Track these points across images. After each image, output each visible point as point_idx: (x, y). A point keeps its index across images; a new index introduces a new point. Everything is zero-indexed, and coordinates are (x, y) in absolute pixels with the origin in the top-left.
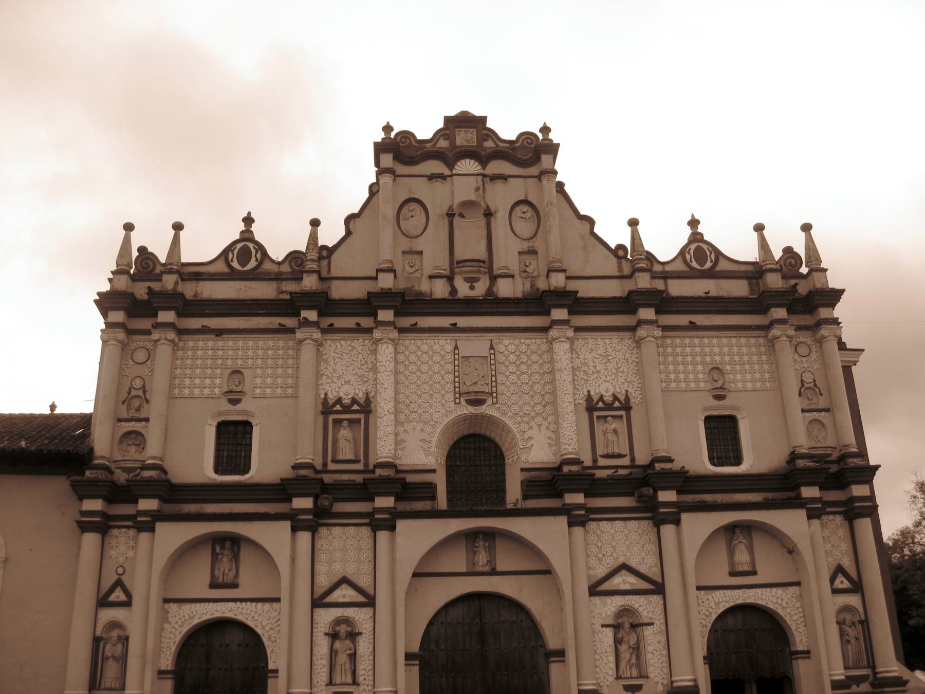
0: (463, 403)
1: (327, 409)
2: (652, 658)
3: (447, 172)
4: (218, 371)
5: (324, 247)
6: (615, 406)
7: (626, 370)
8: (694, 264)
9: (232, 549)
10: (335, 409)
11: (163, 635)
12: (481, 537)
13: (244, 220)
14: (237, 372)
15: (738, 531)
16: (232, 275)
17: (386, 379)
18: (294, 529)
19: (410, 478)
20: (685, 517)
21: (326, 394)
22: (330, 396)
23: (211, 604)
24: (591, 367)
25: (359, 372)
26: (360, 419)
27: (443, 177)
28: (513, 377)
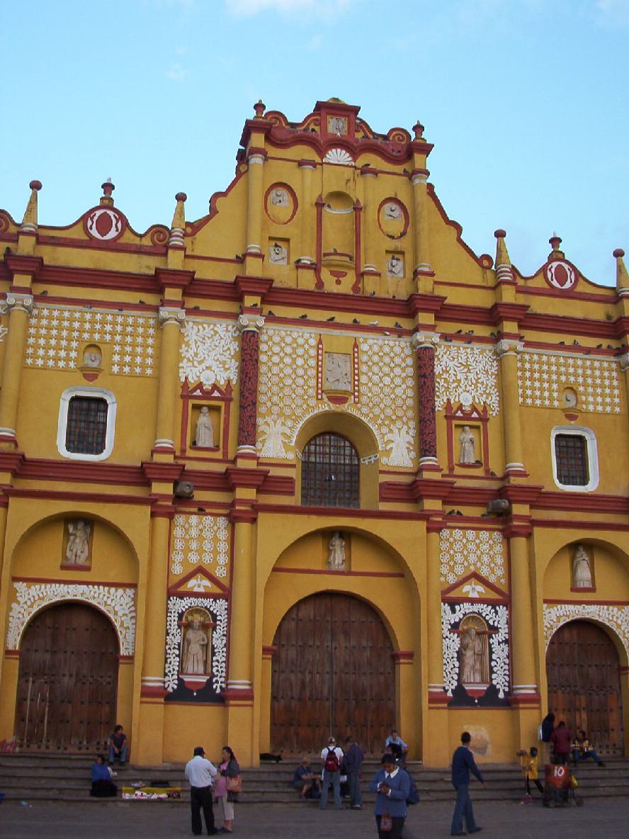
0: (326, 400)
1: (187, 392)
2: (496, 666)
3: (318, 160)
4: (74, 344)
5: (188, 224)
6: (473, 416)
7: (485, 383)
8: (555, 283)
9: (85, 531)
10: (195, 394)
11: (11, 614)
12: (337, 536)
13: (104, 186)
14: (93, 346)
15: (581, 549)
16: (91, 244)
18: (153, 515)
19: (274, 472)
20: (537, 531)
21: (186, 378)
22: (190, 379)
23: (62, 585)
24: (452, 375)
25: (222, 358)
26: (218, 409)
27: (314, 165)
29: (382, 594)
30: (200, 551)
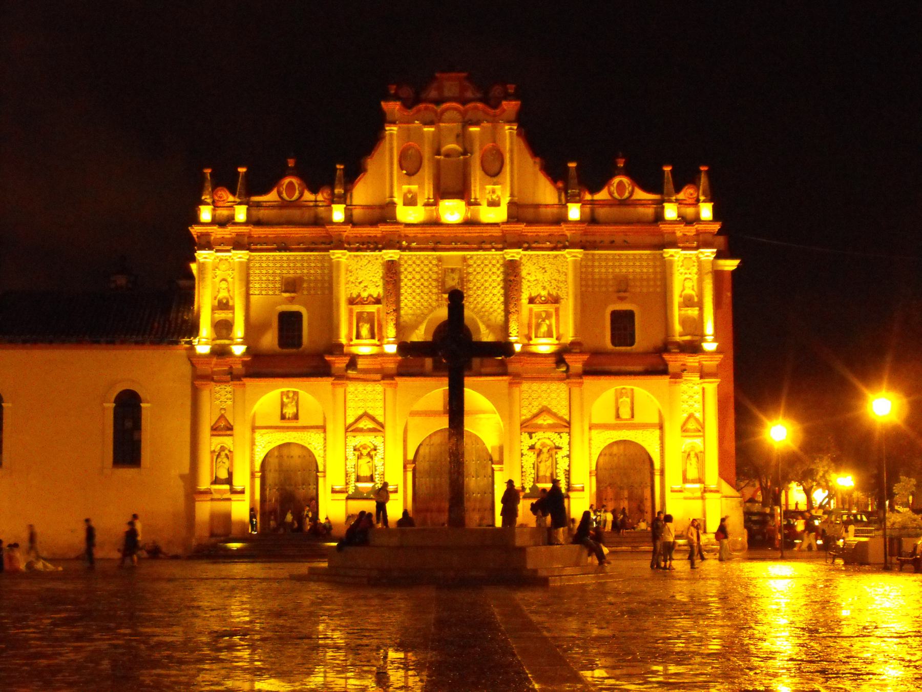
8: (616, 195)
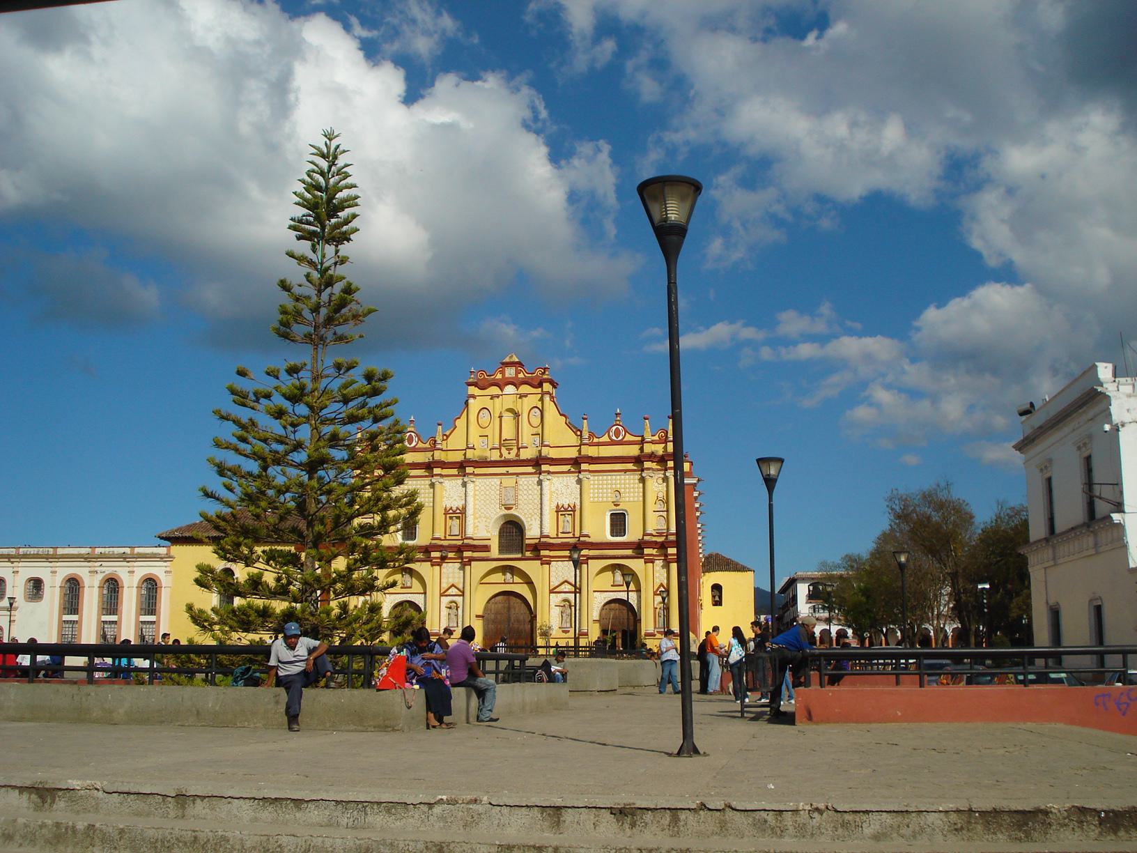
0: (503, 509)
8: (614, 438)
17: (470, 500)
27: (498, 396)
28: (525, 497)
29: (524, 590)
30: (454, 578)
